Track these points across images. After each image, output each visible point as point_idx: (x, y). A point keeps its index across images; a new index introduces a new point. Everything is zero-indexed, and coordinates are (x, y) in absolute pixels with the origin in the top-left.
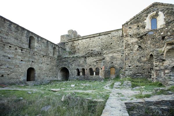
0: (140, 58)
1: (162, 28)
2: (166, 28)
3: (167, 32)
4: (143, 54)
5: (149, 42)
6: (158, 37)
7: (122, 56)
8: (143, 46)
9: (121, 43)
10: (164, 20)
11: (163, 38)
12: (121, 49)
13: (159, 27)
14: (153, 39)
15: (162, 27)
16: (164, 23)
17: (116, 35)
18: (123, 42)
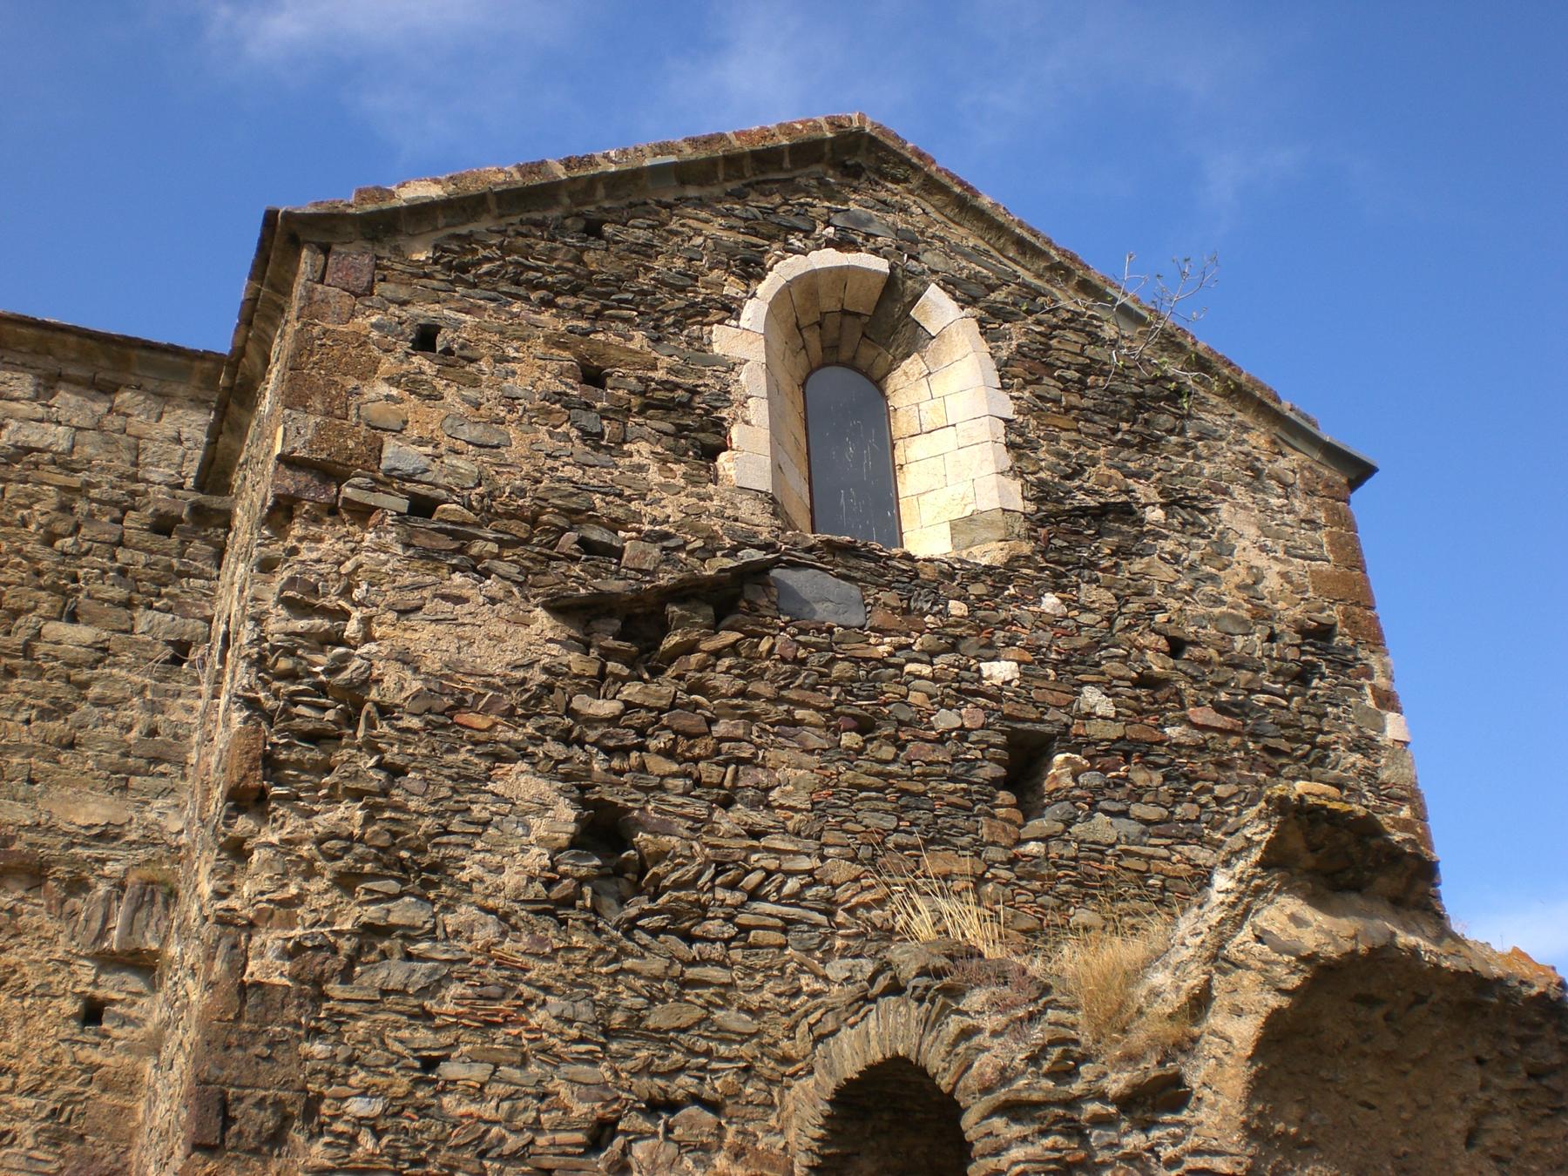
0: (601, 1133)
1: (999, 576)
2: (1050, 602)
3: (1076, 665)
4: (661, 1037)
5: (792, 776)
6: (946, 720)
7: (92, 1012)
8: (669, 834)
9: (124, 676)
10: (1010, 446)
11: (1024, 762)
12: (95, 810)
13: (926, 536)
14: (865, 726)
15: (990, 553)
16: (1014, 496)
17: (58, 437)
18: (181, 650)
